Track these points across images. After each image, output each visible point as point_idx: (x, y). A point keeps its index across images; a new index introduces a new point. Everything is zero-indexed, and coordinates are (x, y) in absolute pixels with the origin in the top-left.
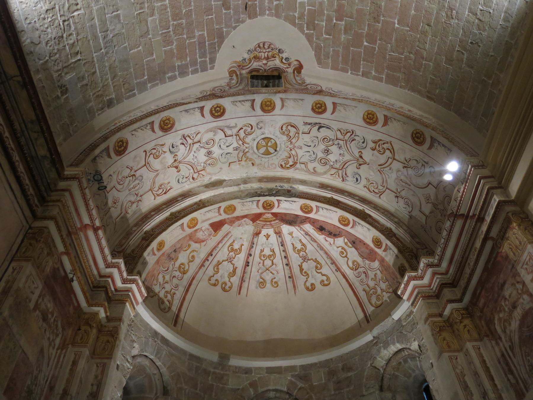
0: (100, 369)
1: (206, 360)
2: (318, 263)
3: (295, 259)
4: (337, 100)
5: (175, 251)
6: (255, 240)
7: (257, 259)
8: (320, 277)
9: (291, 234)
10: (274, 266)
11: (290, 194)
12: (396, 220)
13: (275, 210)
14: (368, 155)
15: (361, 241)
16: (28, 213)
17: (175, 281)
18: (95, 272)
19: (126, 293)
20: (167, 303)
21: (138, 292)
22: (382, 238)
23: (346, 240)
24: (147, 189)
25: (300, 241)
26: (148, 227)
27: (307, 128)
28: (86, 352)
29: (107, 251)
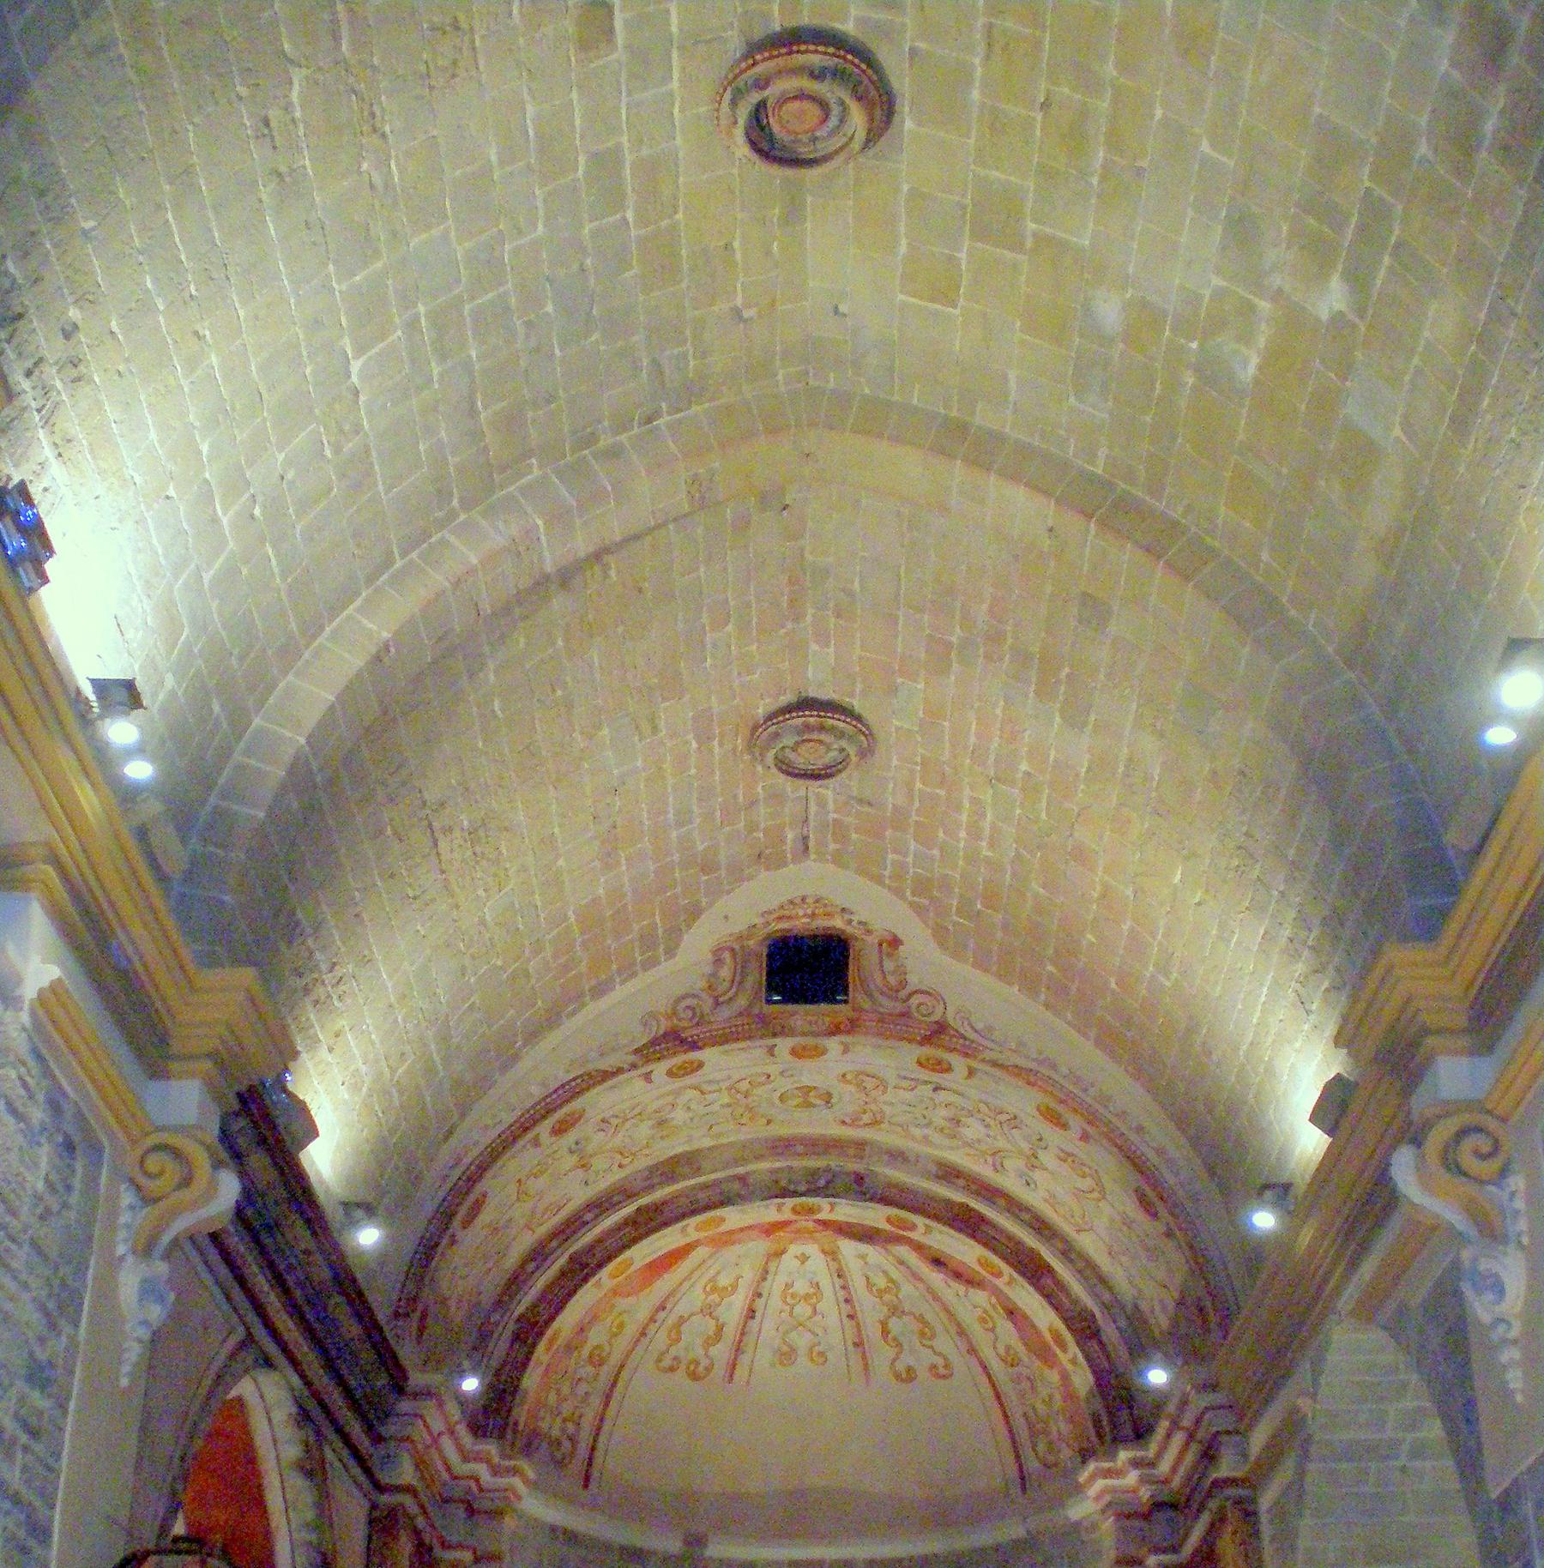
1: (655, 1553)
2: (926, 1324)
3: (871, 1311)
4: (974, 1064)
5: (582, 1330)
6: (772, 1266)
7: (775, 1302)
8: (927, 1357)
9: (863, 1257)
10: (818, 1318)
11: (861, 1187)
12: (1107, 1297)
13: (824, 1215)
14: (1047, 1158)
15: (1025, 1317)
16: (367, 1485)
17: (582, 1388)
18: (445, 1475)
22: (1068, 1337)
23: (994, 1300)
25: (885, 1273)
27: (906, 1084)
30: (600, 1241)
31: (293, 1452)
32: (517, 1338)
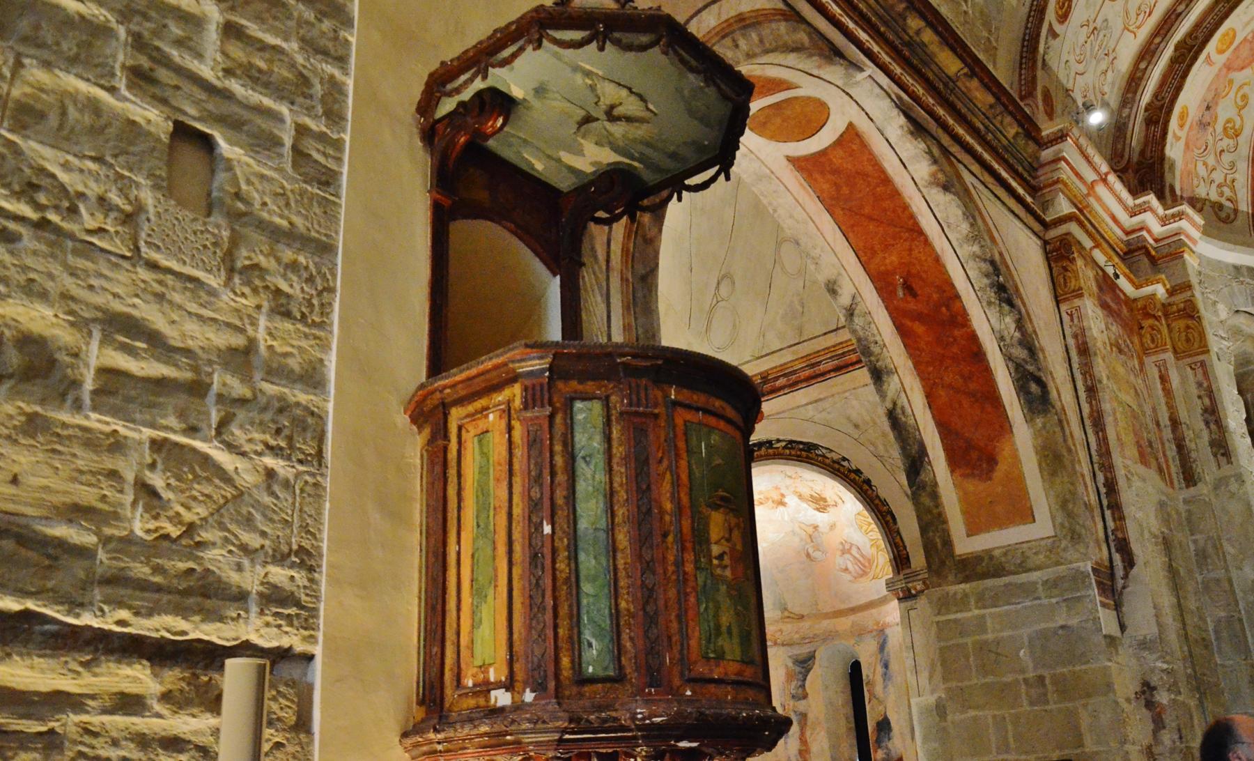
0: (1200, 371)
5: (1208, 108)
16: (1037, 227)
17: (1226, 158)
18: (1119, 233)
19: (1176, 238)
20: (1228, 204)
21: (1191, 225)
24: (1119, 32)
26: (1146, 97)
28: (1169, 356)
29: (1125, 194)
30: (1197, 25)
31: (923, 169)
32: (1150, 122)
